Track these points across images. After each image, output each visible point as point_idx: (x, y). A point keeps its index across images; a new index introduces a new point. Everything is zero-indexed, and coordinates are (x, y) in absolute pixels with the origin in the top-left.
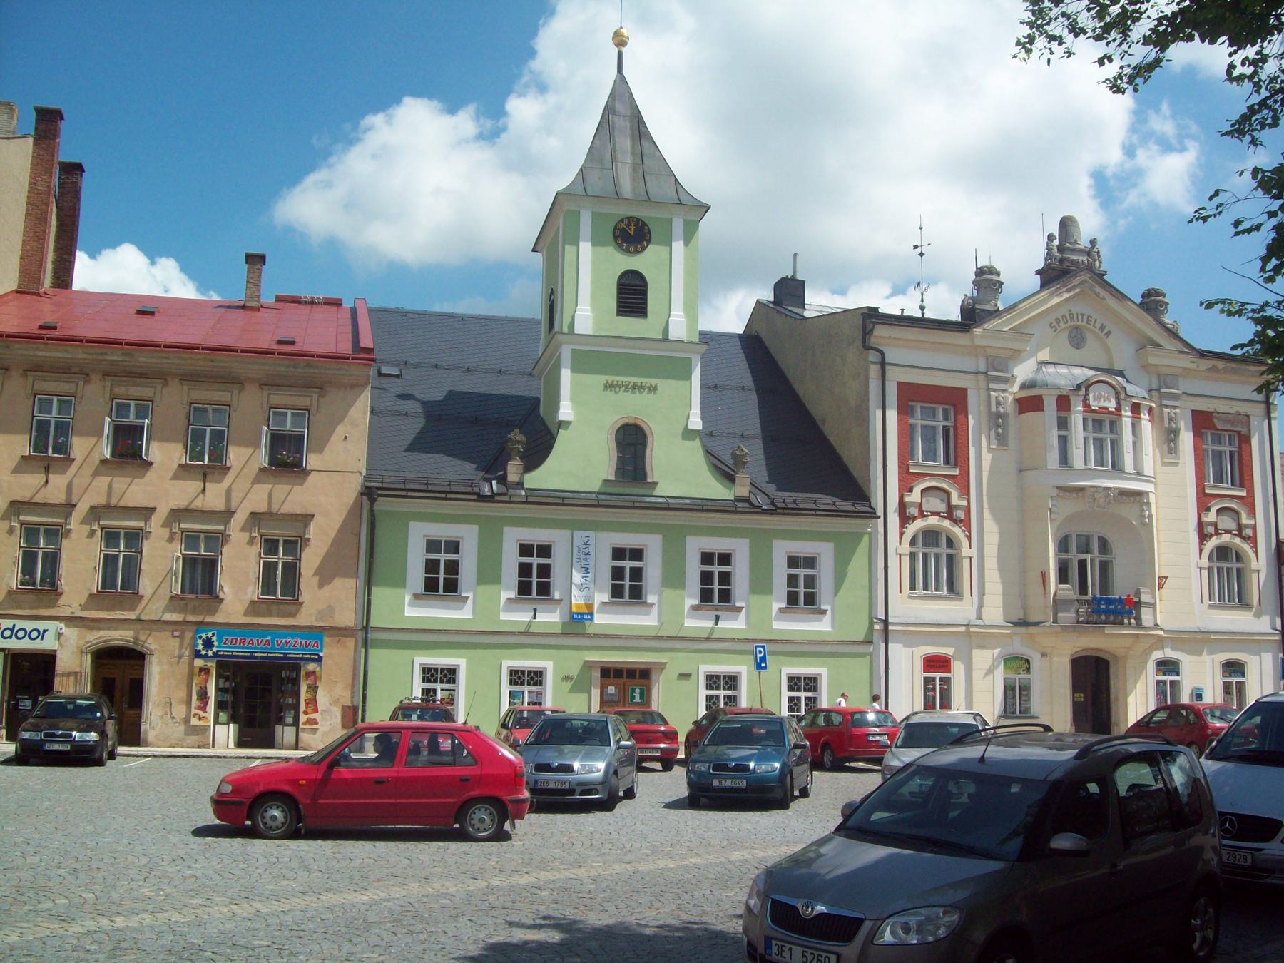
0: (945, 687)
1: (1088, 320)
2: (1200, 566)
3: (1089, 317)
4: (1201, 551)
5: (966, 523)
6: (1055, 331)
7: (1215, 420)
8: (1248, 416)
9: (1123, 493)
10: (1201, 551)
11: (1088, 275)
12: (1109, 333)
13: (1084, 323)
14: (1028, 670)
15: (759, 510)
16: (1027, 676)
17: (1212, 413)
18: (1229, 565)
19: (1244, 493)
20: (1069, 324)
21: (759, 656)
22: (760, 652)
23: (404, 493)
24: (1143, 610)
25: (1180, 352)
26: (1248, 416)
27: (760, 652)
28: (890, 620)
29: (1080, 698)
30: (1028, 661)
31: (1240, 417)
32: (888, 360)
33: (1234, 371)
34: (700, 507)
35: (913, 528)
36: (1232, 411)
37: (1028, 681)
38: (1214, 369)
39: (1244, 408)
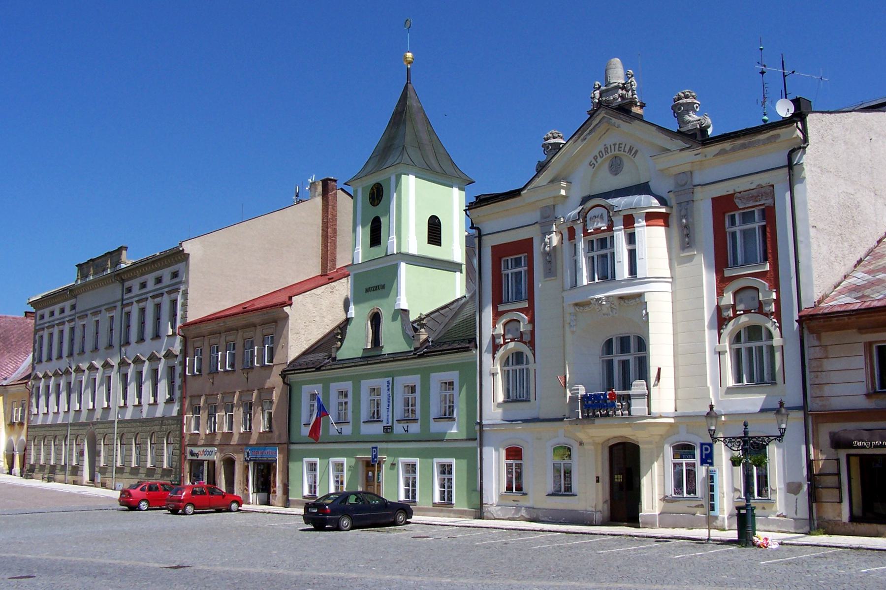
0: (519, 471)
1: (619, 147)
2: (718, 350)
3: (620, 144)
4: (720, 335)
5: (532, 344)
6: (593, 168)
7: (736, 201)
8: (773, 186)
9: (622, 298)
10: (720, 335)
11: (603, 112)
12: (636, 152)
13: (617, 152)
14: (570, 456)
15: (314, 369)
16: (569, 461)
17: (733, 195)
18: (758, 344)
19: (767, 267)
20: (610, 154)
21: (374, 454)
22: (375, 451)
23: (293, 372)
24: (633, 401)
25: (681, 150)
26: (773, 186)
27: (375, 451)
28: (484, 422)
29: (619, 478)
30: (569, 449)
31: (763, 190)
32: (483, 232)
33: (744, 147)
34: (392, 359)
35: (499, 354)
36: (753, 186)
37: (570, 465)
38: (723, 152)
39: (764, 179)
